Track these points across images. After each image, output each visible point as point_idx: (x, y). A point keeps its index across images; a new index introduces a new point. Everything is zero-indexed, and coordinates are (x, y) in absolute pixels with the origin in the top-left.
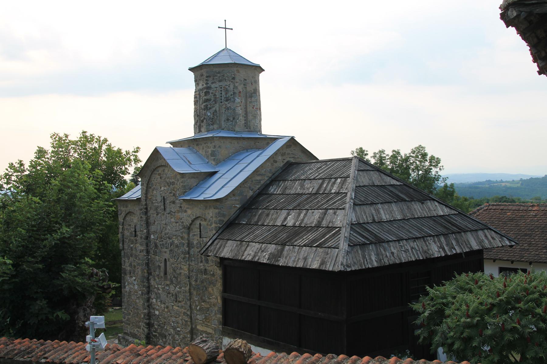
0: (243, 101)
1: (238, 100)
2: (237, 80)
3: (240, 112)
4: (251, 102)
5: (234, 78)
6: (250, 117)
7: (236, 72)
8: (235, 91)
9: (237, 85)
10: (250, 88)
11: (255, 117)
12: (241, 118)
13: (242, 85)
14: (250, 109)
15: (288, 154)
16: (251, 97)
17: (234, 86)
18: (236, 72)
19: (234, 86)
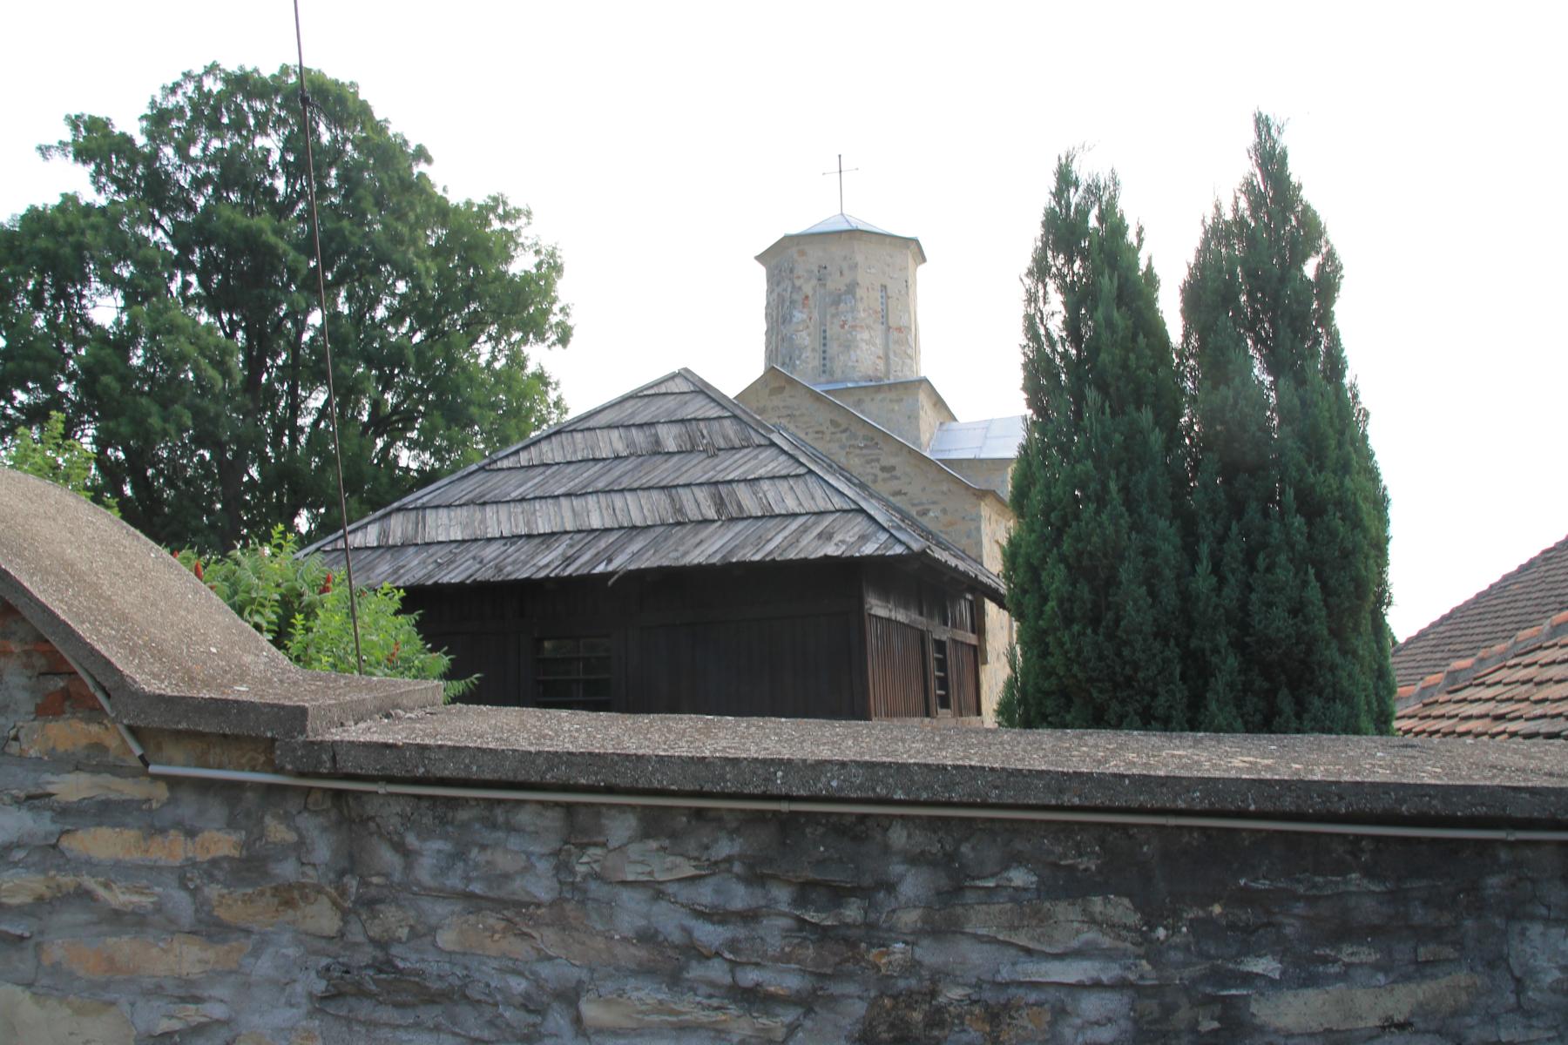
0: (816, 315)
1: (799, 316)
2: (800, 271)
3: (807, 341)
4: (833, 316)
5: (791, 271)
6: (833, 349)
7: (796, 256)
8: (795, 297)
9: (798, 283)
10: (836, 283)
11: (848, 348)
12: (808, 354)
13: (814, 282)
14: (833, 330)
15: (775, 408)
16: (837, 301)
17: (794, 286)
18: (796, 256)
19: (794, 286)
